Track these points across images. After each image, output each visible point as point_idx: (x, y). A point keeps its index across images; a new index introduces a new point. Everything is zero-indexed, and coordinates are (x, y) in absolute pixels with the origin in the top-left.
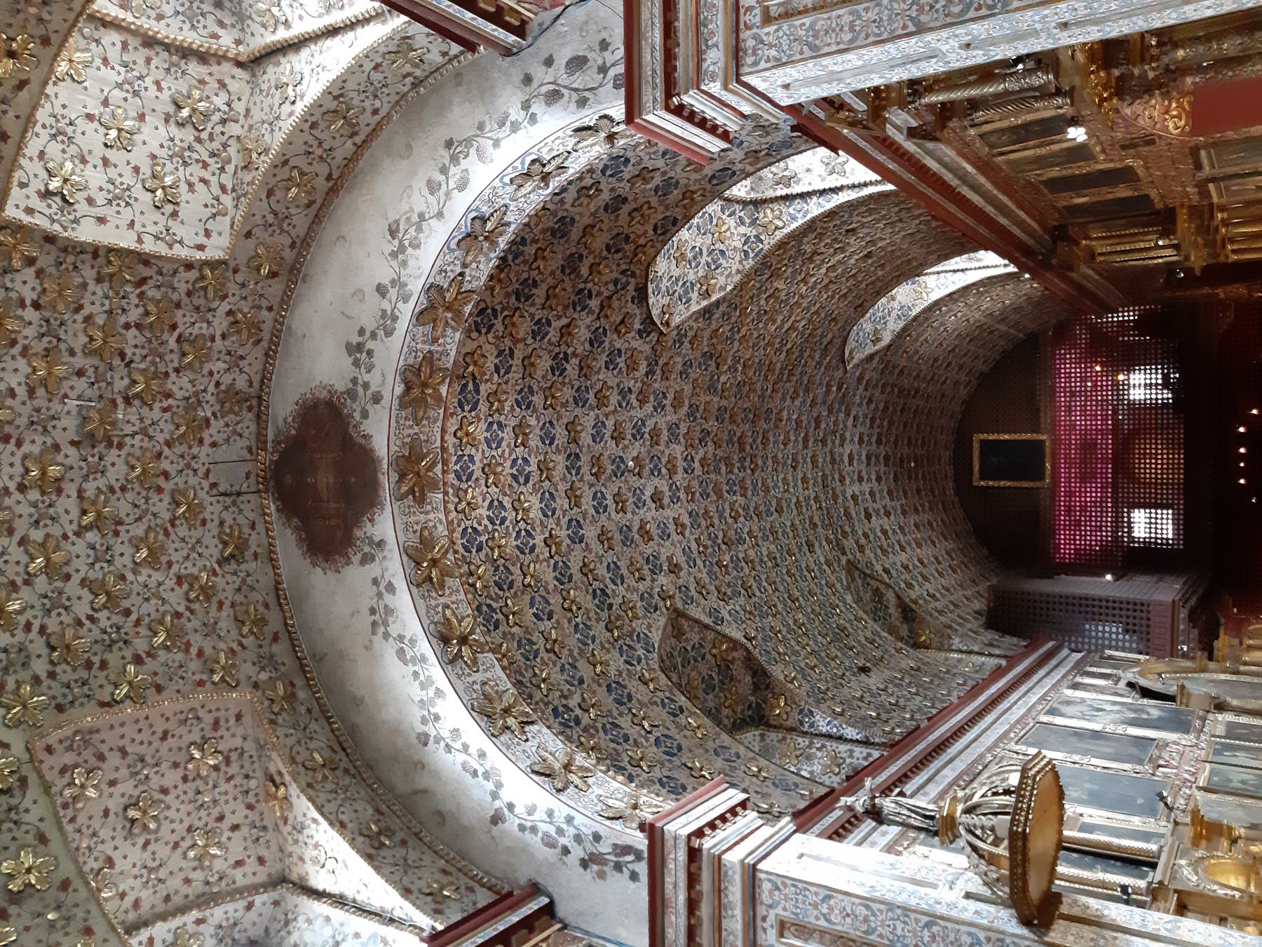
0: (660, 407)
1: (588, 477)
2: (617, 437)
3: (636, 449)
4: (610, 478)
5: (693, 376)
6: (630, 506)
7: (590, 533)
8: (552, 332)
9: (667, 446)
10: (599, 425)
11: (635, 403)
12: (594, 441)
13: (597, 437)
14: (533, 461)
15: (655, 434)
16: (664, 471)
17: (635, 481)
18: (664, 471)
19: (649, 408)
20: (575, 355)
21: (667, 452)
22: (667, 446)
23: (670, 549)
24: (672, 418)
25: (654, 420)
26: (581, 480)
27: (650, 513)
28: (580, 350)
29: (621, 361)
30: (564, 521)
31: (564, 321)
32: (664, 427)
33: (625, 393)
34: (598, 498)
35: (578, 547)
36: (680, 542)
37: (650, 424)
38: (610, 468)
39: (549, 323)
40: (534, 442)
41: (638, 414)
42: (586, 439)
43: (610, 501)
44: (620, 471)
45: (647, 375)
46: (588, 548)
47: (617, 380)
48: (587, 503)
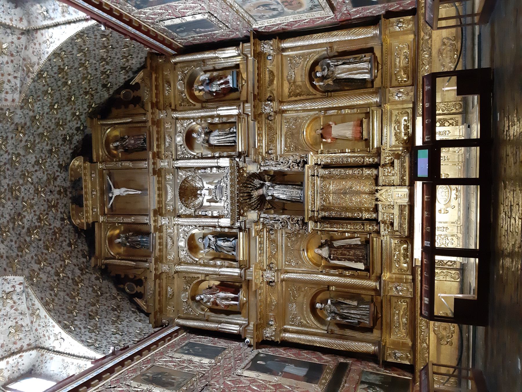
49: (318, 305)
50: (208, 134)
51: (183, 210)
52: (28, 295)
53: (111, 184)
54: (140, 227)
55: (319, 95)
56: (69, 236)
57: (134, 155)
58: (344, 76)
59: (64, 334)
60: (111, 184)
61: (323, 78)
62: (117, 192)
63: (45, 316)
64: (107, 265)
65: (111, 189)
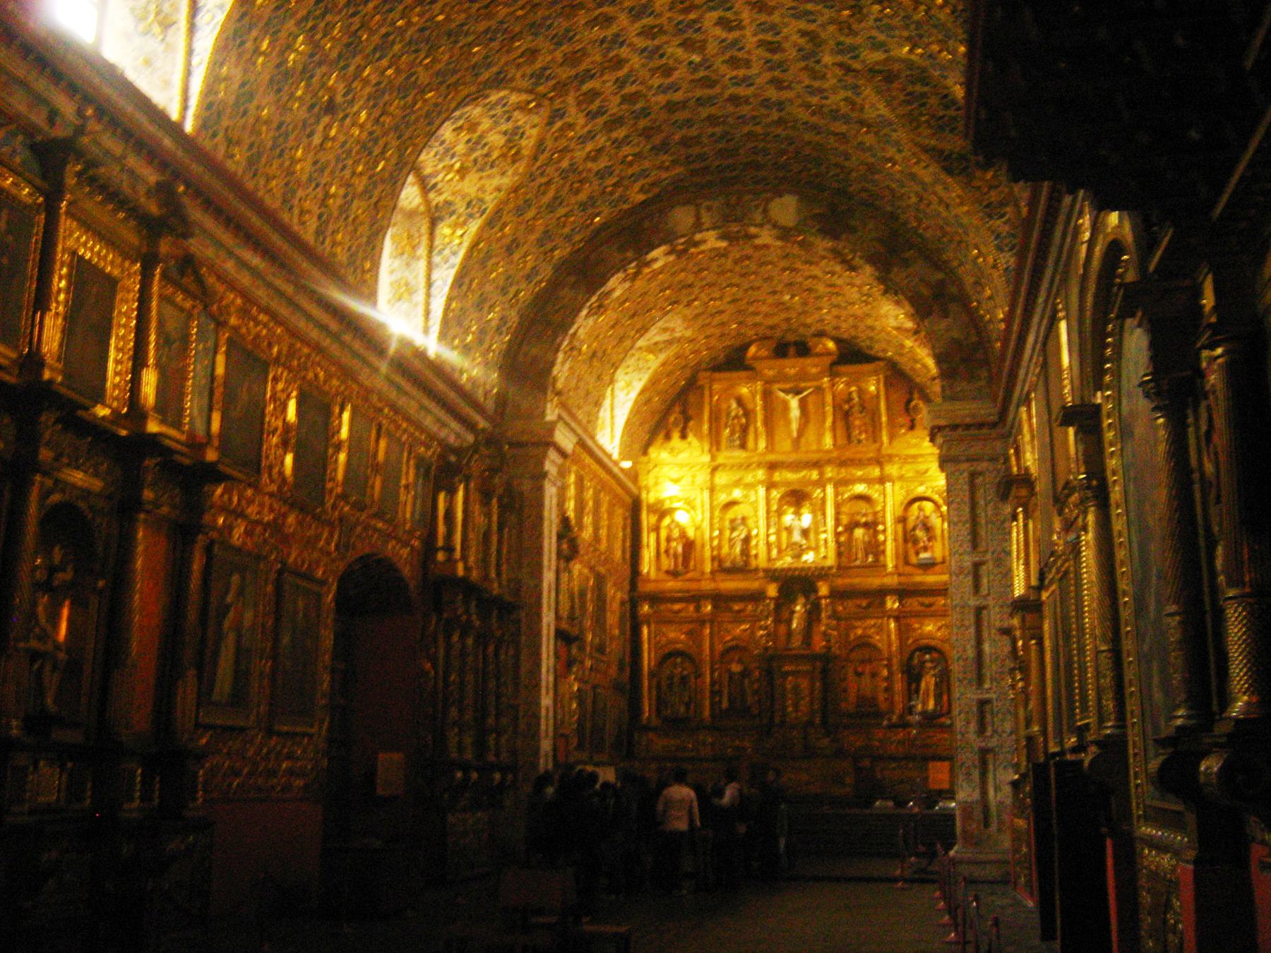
0: (617, 40)
1: (717, 90)
2: (667, 71)
3: (674, 50)
4: (714, 71)
5: (565, 24)
6: (740, 55)
7: (772, 94)
8: (602, 165)
9: (660, 15)
10: (663, 89)
11: (626, 70)
12: (679, 88)
13: (674, 87)
14: (710, 131)
15: (648, 33)
16: (692, 16)
17: (712, 48)
18: (692, 16)
19: (624, 52)
20: (609, 139)
21: (669, 15)
22: (660, 15)
23: (792, 31)
24: (623, 19)
25: (635, 40)
26: (721, 94)
27: (751, 40)
28: (603, 139)
29: (594, 106)
30: (763, 111)
31: (590, 165)
32: (638, 25)
33: (621, 83)
34: (737, 82)
35: (788, 109)
36: (783, 16)
37: (641, 43)
38: (701, 74)
39: (597, 173)
40: (693, 132)
41: (636, 61)
42: (678, 96)
43: (741, 72)
44: (706, 64)
45: (592, 77)
46: (790, 101)
47: (611, 98)
48: (742, 91)
49: (679, 660)
50: (866, 525)
51: (776, 494)
52: (669, 343)
53: (805, 393)
54: (752, 429)
55: (907, 656)
56: (738, 343)
57: (840, 424)
58: (923, 685)
59: (634, 395)
60: (805, 393)
61: (923, 663)
62: (794, 403)
63: (649, 368)
64: (702, 387)
65: (797, 393)
